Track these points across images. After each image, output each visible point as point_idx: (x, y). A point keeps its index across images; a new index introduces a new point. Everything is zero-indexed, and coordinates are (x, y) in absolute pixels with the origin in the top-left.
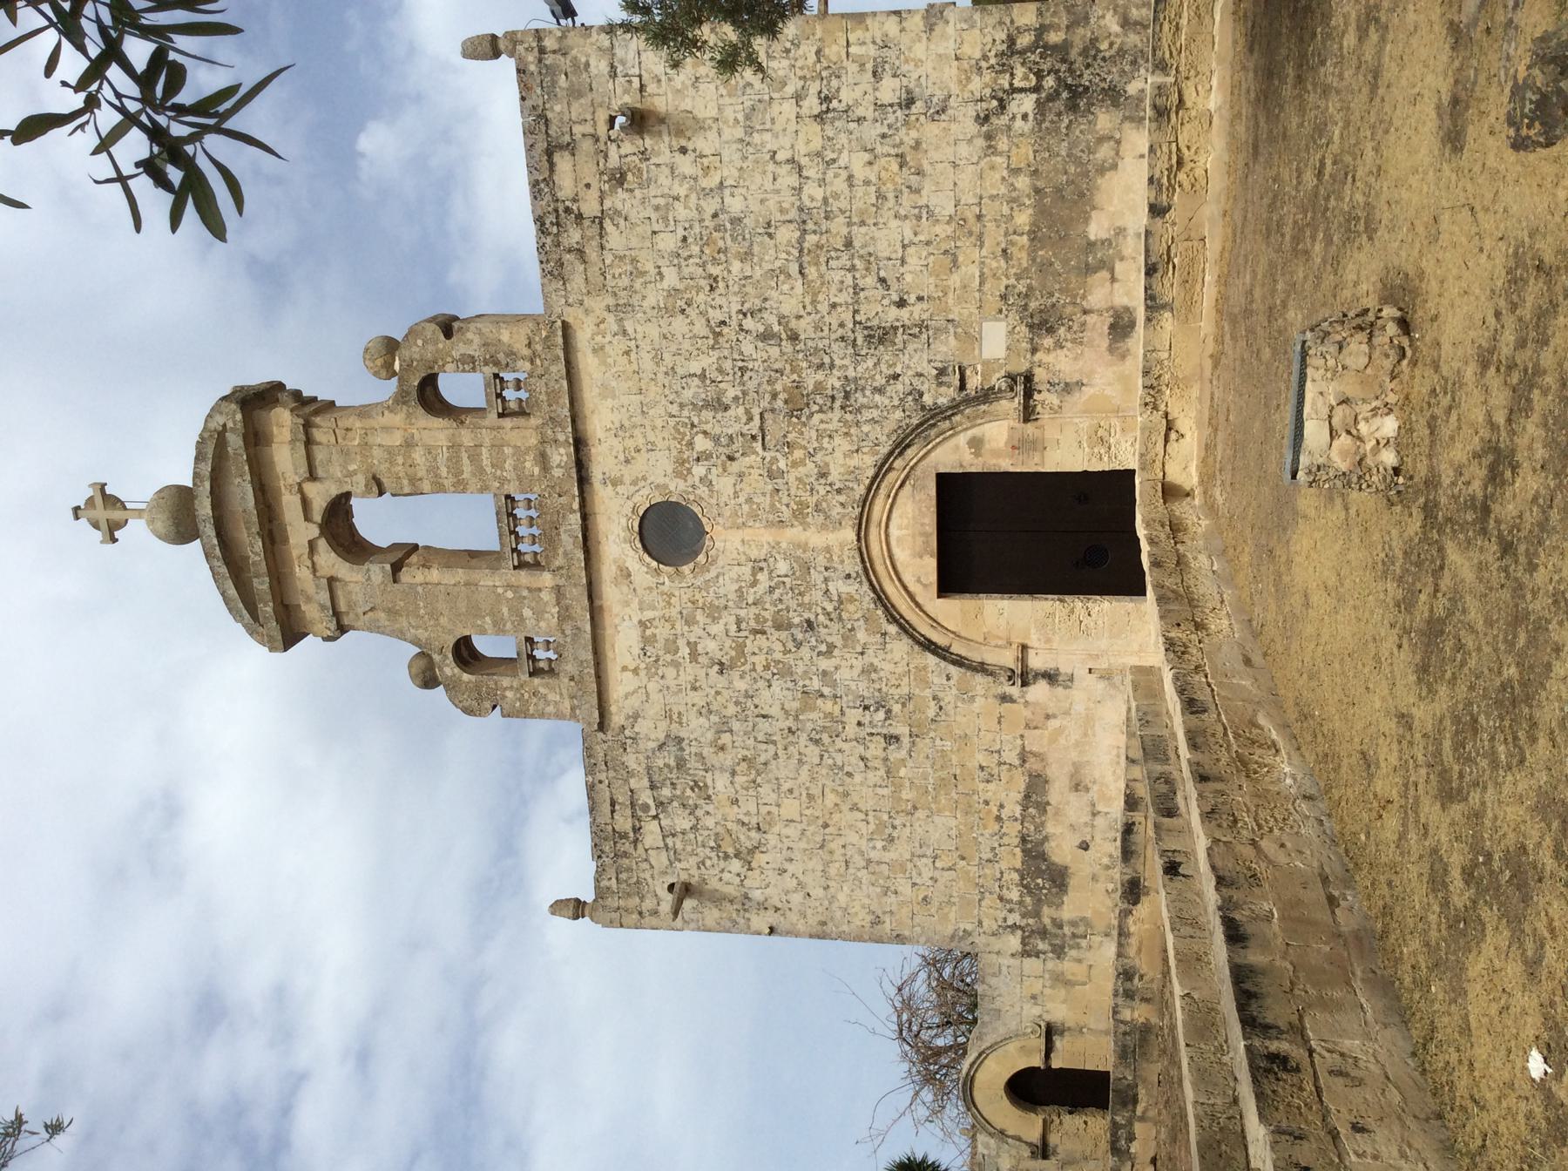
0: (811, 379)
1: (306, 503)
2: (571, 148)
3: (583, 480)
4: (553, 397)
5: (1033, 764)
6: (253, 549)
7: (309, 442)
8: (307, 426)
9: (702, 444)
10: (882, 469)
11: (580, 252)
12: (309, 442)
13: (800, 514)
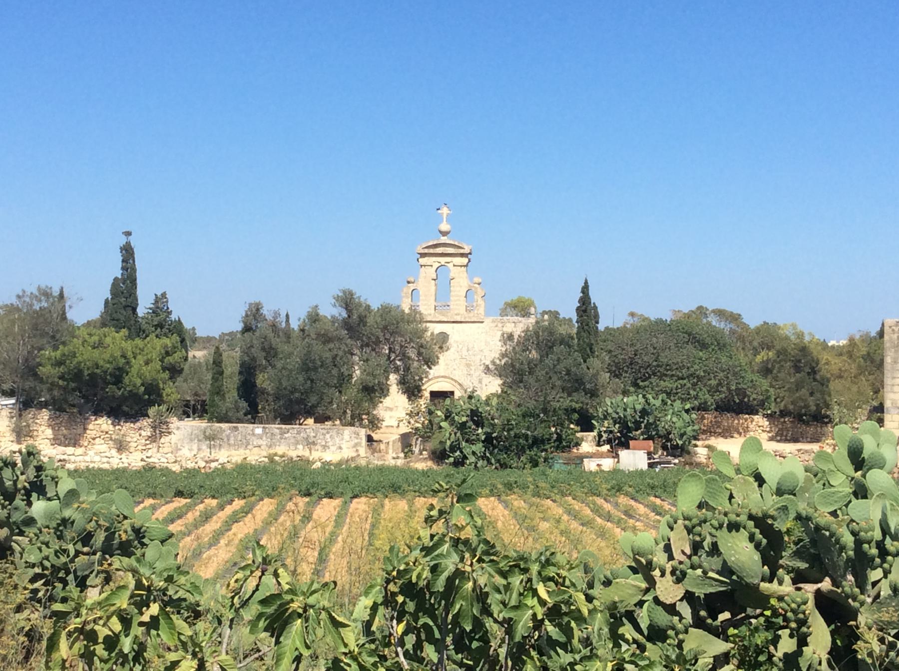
0: (473, 368)
1: (448, 263)
2: (515, 327)
3: (454, 322)
4: (470, 317)
5: (395, 409)
6: (439, 250)
7: (461, 266)
8: (464, 266)
9: (460, 346)
10: (456, 381)
11: (496, 326)
12: (461, 266)
13: (446, 365)
